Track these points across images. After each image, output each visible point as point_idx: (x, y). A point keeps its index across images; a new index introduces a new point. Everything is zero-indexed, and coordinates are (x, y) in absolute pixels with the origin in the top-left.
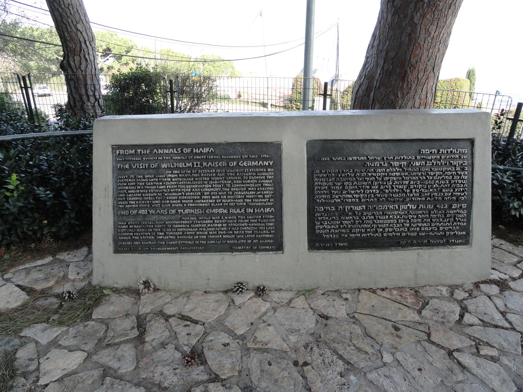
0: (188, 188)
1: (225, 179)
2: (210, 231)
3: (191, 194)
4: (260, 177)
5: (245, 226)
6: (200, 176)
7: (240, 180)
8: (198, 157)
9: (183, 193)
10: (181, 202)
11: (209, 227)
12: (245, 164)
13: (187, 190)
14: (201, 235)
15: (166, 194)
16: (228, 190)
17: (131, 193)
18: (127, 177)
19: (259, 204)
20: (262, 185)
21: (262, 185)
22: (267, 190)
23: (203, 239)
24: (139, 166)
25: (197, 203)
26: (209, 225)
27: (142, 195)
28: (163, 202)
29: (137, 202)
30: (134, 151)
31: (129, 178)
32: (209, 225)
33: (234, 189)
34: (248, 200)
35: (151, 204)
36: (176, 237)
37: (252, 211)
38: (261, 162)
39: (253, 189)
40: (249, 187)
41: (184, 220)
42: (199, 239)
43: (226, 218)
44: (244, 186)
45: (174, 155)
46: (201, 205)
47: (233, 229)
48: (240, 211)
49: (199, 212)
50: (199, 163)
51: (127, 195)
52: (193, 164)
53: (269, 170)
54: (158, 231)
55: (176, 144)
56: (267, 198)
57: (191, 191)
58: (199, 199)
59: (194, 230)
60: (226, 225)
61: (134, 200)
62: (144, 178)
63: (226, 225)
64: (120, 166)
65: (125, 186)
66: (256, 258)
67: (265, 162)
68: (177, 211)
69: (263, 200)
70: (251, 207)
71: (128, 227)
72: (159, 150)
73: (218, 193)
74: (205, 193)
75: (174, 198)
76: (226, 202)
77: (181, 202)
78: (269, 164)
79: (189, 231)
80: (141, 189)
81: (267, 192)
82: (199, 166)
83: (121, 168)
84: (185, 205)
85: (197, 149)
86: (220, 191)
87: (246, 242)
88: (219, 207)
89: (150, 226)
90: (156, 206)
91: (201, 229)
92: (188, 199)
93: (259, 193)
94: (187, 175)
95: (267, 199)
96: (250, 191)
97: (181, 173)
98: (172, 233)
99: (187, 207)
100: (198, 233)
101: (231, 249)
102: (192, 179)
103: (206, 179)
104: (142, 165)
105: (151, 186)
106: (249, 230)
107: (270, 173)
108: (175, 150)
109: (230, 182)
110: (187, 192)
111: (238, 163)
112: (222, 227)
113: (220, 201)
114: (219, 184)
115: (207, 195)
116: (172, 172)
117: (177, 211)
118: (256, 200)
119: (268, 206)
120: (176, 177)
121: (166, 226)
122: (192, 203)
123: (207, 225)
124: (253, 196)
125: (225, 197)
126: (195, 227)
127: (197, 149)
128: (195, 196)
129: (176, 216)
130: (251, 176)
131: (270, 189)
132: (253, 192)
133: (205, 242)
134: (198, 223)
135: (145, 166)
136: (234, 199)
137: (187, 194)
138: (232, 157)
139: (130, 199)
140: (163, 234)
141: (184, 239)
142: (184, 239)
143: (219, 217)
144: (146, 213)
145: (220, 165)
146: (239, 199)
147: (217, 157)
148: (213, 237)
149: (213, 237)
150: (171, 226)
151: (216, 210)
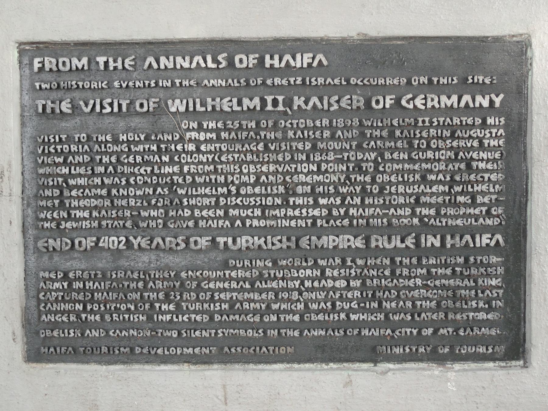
0: (249, 174)
1: (359, 147)
2: (313, 301)
3: (257, 190)
4: (462, 143)
5: (416, 287)
6: (285, 139)
7: (403, 150)
8: (277, 81)
9: (233, 189)
10: (226, 213)
11: (307, 290)
12: (419, 102)
13: (245, 179)
14: (285, 312)
15: (181, 191)
16: (368, 179)
17: (78, 187)
18: (64, 137)
19: (459, 222)
20: (469, 166)
21: (469, 166)
22: (483, 182)
23: (291, 325)
24: (102, 107)
25: (275, 217)
26: (308, 284)
27: (109, 192)
28: (172, 213)
29: (95, 214)
30: (85, 60)
31: (70, 140)
32: (308, 284)
33: (386, 178)
34: (425, 211)
35: (136, 220)
36: (212, 318)
37: (437, 244)
38: (467, 98)
39: (441, 176)
40: (431, 171)
41: (235, 268)
42: (278, 325)
43: (360, 262)
44: (416, 167)
45: (204, 73)
46: (286, 223)
47: (379, 294)
48: (402, 241)
49: (279, 245)
50: (280, 98)
51: (66, 193)
52: (263, 102)
53: (490, 121)
54: (158, 300)
55: (211, 42)
56: (483, 204)
57: (257, 182)
58: (279, 207)
59: (264, 296)
60: (358, 283)
61: (85, 208)
62: (116, 141)
63: (358, 283)
64: (44, 107)
65: (57, 165)
66: (448, 380)
67: (479, 99)
68: (213, 241)
69: (472, 211)
70: (434, 231)
71: (70, 285)
72: (163, 60)
73: (335, 188)
74: (299, 190)
75: (206, 201)
76: (361, 217)
77: (226, 213)
78: (492, 102)
79: (250, 301)
80: (105, 174)
81: (484, 188)
82: (281, 108)
83: (49, 110)
84: (238, 222)
85: (276, 57)
86: (345, 184)
87: (419, 333)
88: (338, 231)
89: (133, 285)
90: (153, 224)
91: (286, 295)
92: (248, 207)
93: (459, 189)
94: (245, 134)
95: (484, 209)
96: (432, 184)
97: (226, 129)
98: (198, 306)
99: (246, 230)
100: (275, 307)
101: (371, 353)
102: (261, 147)
103: (300, 146)
104: (111, 105)
105: (135, 164)
106: (426, 299)
107: (494, 131)
108: (209, 58)
109: (373, 155)
110: (245, 184)
111: (398, 101)
112: (348, 288)
113: (342, 211)
114: (341, 161)
115: (304, 195)
116: (200, 125)
117: (213, 241)
118: (451, 211)
119: (485, 229)
120: (211, 141)
121: (182, 285)
122: (259, 218)
123: (302, 283)
124: (440, 200)
125: (358, 201)
126: (267, 290)
127: (276, 57)
128: (267, 196)
129: (212, 255)
130: (438, 138)
131: (493, 177)
132: (441, 188)
133: (296, 333)
134: (275, 278)
135: (120, 106)
136: (384, 206)
137: (243, 192)
138: (381, 81)
139: (75, 203)
140: (172, 307)
141: (233, 325)
142: (233, 325)
143: (338, 261)
144: (121, 246)
145: (343, 105)
146: (401, 206)
147: (337, 81)
148: (321, 317)
149: (321, 317)
150: (195, 284)
151: (331, 237)
